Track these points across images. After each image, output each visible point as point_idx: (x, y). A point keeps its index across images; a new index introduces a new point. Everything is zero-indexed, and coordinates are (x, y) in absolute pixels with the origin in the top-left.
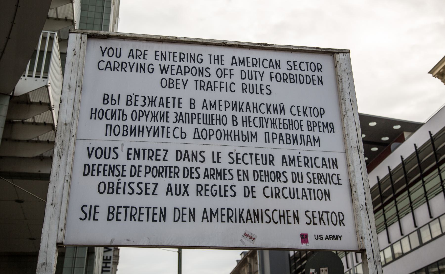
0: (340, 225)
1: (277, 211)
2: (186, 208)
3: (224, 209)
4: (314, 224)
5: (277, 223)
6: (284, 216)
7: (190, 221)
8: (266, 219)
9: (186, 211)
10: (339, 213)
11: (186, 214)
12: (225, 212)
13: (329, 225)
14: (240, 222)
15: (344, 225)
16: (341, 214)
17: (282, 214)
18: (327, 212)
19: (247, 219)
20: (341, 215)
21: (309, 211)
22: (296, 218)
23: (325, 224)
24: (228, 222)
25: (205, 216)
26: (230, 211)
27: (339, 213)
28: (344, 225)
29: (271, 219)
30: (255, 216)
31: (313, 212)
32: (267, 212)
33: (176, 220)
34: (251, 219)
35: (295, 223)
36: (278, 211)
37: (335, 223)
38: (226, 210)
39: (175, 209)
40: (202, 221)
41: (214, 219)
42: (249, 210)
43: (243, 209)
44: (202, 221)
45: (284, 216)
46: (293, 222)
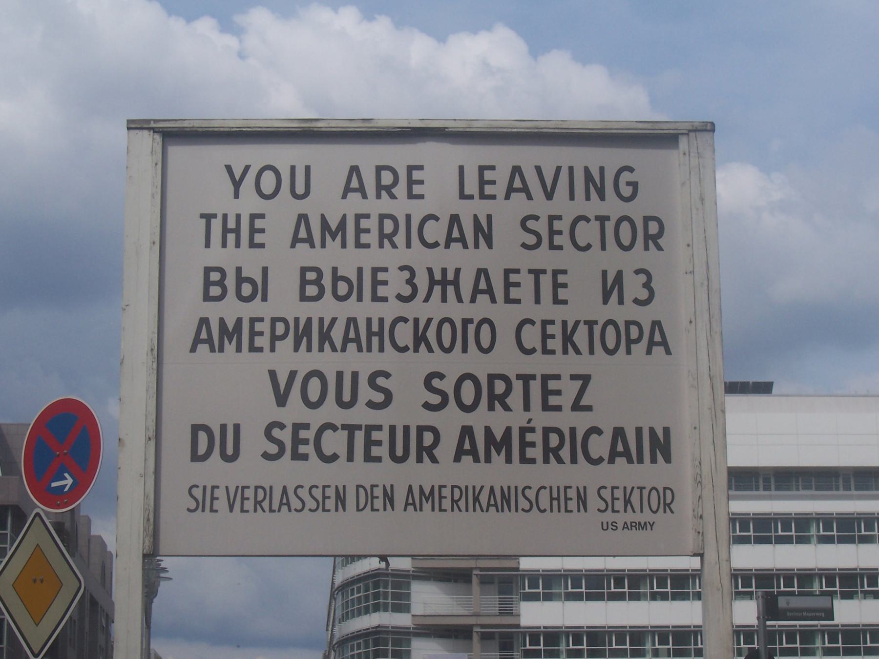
0: (665, 512)
1: (545, 488)
2: (377, 486)
3: (445, 486)
4: (614, 511)
5: (545, 511)
6: (559, 499)
7: (385, 509)
8: (523, 504)
9: (378, 492)
10: (665, 489)
11: (377, 497)
12: (446, 492)
13: (642, 512)
14: (474, 510)
15: (672, 512)
16: (668, 492)
17: (555, 495)
18: (641, 489)
19: (489, 505)
20: (668, 492)
21: (605, 488)
22: (582, 500)
23: (634, 512)
24: (453, 510)
25: (410, 501)
26: (457, 491)
27: (665, 489)
28: (672, 512)
29: (534, 505)
30: (504, 500)
31: (613, 488)
32: (527, 492)
33: (361, 507)
34: (496, 505)
35: (579, 511)
36: (548, 489)
37: (654, 509)
38: (449, 489)
39: (358, 487)
40: (405, 510)
41: (427, 506)
42: (492, 488)
43: (482, 487)
44: (405, 510)
45: (558, 499)
46: (575, 509)
